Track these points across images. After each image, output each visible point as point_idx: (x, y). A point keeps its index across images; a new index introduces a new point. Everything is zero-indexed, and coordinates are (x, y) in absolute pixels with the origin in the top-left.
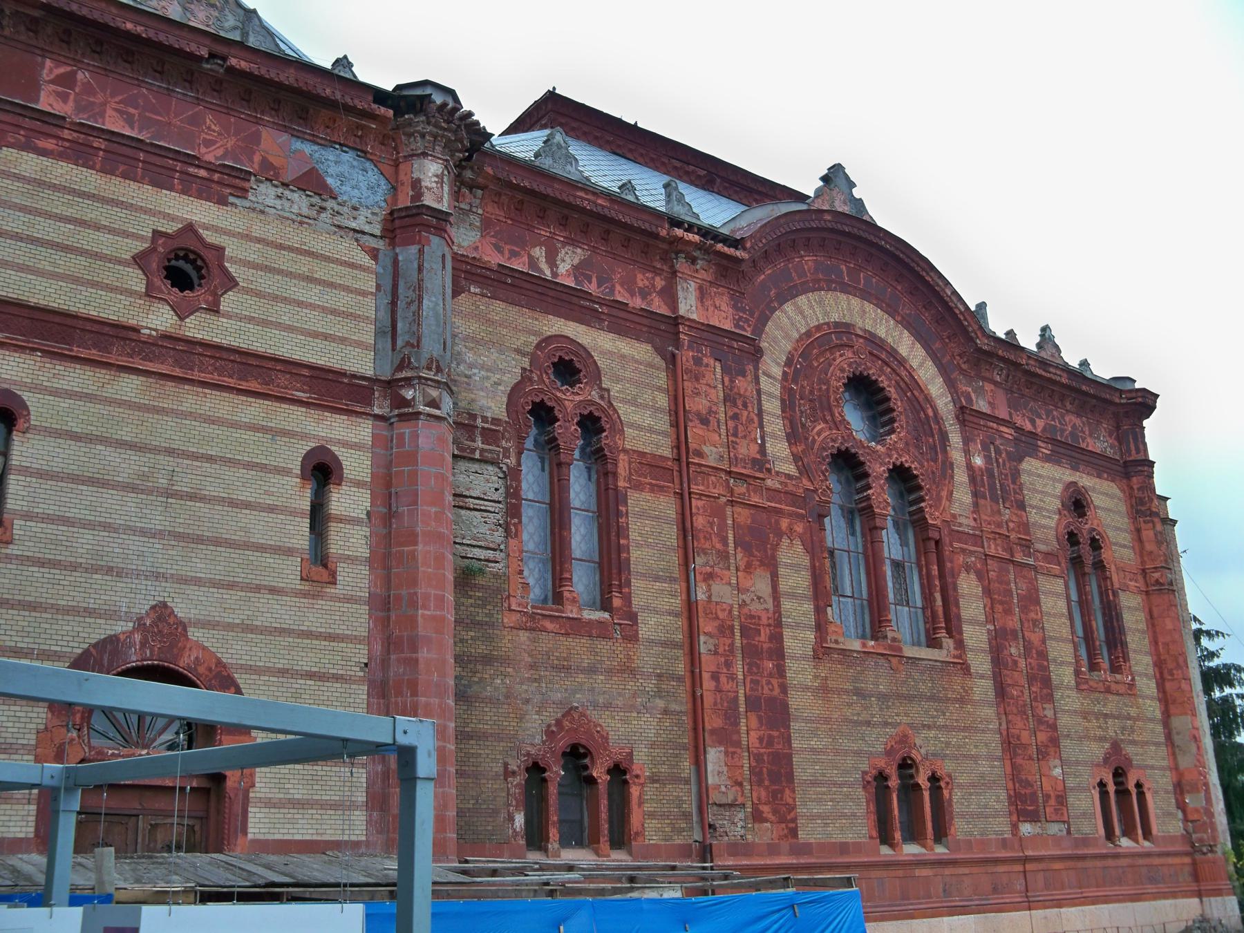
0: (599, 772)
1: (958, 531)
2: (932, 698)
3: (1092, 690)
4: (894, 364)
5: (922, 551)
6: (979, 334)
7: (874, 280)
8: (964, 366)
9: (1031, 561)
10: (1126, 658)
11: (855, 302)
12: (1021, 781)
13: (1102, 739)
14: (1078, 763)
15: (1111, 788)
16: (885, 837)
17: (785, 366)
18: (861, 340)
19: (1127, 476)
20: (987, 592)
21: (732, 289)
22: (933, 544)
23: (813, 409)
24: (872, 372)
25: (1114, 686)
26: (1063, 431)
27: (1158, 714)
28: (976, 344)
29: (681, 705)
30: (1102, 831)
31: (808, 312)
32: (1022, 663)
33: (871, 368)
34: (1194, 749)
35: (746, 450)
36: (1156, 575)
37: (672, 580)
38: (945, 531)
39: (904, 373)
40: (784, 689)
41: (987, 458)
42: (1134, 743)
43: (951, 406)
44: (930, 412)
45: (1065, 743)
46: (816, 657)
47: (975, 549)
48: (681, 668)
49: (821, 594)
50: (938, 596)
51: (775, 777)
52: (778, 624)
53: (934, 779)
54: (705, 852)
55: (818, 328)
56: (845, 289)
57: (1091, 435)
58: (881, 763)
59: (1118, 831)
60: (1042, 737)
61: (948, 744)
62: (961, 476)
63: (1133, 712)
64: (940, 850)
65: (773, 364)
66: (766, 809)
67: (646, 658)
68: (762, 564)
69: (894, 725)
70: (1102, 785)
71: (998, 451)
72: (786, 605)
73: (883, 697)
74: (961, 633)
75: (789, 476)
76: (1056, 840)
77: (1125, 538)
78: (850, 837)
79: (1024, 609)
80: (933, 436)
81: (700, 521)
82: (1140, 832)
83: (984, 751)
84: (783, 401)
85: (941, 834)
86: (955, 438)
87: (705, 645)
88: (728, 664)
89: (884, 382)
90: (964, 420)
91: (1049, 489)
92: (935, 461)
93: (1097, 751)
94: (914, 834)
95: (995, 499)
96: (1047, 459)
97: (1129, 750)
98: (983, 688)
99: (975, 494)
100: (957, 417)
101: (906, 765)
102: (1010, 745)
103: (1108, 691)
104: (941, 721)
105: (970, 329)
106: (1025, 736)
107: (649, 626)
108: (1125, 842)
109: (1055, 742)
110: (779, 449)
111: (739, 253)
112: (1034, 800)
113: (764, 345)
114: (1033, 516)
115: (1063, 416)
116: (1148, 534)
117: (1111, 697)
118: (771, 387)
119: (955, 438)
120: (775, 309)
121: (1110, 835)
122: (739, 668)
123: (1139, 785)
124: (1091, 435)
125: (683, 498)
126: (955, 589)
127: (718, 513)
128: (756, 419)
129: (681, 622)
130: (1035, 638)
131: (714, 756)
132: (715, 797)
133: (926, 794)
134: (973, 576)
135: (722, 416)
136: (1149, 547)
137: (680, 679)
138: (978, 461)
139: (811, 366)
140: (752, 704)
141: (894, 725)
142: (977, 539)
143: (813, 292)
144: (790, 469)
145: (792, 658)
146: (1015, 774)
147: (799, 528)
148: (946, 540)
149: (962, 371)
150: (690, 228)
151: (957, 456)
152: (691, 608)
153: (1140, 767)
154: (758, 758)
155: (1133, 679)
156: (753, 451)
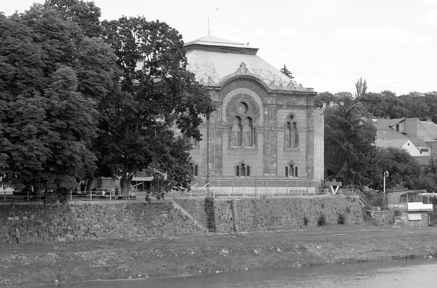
0: (194, 167)
2: (249, 154)
3: (287, 151)
5: (252, 130)
9: (276, 130)
10: (298, 145)
11: (243, 89)
12: (266, 167)
13: (288, 160)
14: (281, 164)
15: (289, 168)
16: (238, 175)
19: (308, 109)
20: (264, 136)
22: (254, 129)
23: (232, 110)
24: (245, 102)
25: (293, 150)
26: (291, 102)
27: (305, 155)
29: (206, 157)
30: (285, 175)
31: (233, 93)
32: (270, 148)
34: (311, 161)
35: (219, 120)
36: (309, 129)
37: (205, 140)
38: (256, 127)
39: (252, 100)
40: (222, 154)
41: (269, 112)
42: (297, 160)
43: (262, 104)
44: (256, 106)
45: (278, 160)
46: (228, 149)
48: (206, 152)
49: (230, 140)
50: (253, 138)
51: (219, 167)
52: (222, 145)
53: (248, 167)
54: (208, 177)
55: (234, 96)
56: (241, 87)
57: (299, 101)
58: (238, 165)
59: (294, 175)
60: (272, 160)
61: (251, 162)
62: (262, 116)
63: (297, 155)
64: (248, 177)
65: (225, 105)
66: (217, 171)
67: (201, 151)
68: (220, 137)
69: (241, 159)
70: (287, 168)
71: (272, 110)
72: (223, 142)
73: (240, 155)
74: (257, 143)
75: (226, 122)
76: (273, 177)
77: (305, 121)
78: (231, 175)
79: (272, 139)
81: (210, 132)
82: (294, 175)
83: (259, 162)
85: (248, 175)
86: (261, 110)
87: (209, 149)
88: (213, 152)
89: (247, 103)
91: (284, 115)
92: (256, 114)
93: (287, 162)
94: (244, 175)
95: (269, 119)
96: (285, 109)
97: (295, 162)
98: (260, 152)
99: (264, 119)
101: (243, 165)
102: (265, 161)
103: (292, 151)
104: (251, 158)
106: (268, 160)
107: (201, 147)
108: (291, 177)
109: (276, 161)
110: (225, 119)
111: (220, 89)
112: (269, 170)
113: (224, 101)
114: (279, 121)
115: (291, 99)
116: (309, 121)
117: (292, 152)
118: (224, 108)
119: (261, 110)
120: (226, 95)
121: (287, 175)
122: (215, 152)
123: (296, 168)
124: (299, 101)
125: (208, 129)
126: (257, 136)
127: (213, 130)
129: (206, 146)
130: (274, 143)
131: (210, 164)
132: (209, 169)
133: (246, 169)
134: (261, 134)
135: (215, 115)
136: (309, 123)
137: (206, 154)
138: (266, 113)
139: (232, 103)
140: (216, 157)
141: (241, 159)
142: (263, 127)
144: (227, 121)
145: (224, 150)
146: (265, 165)
147: (227, 130)
148: (256, 128)
149: (266, 96)
150: (211, 87)
151: (261, 112)
152: (208, 144)
153: (297, 164)
154: (217, 164)
155: (299, 149)
156: (220, 120)
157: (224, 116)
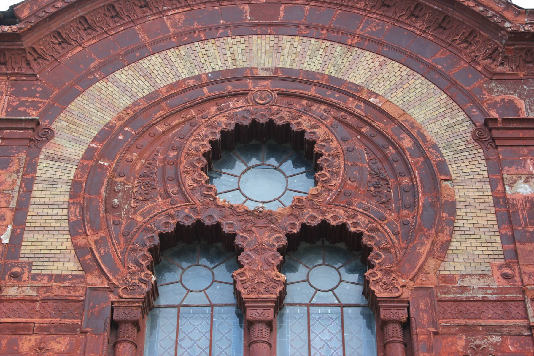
1: (455, 301)
4: (335, 98)
6: (508, 14)
7: (308, 7)
8: (506, 69)
17: (94, 140)
18: (266, 83)
21: (12, 75)
22: (395, 331)
28: (504, 29)
33: (279, 111)
39: (352, 105)
44: (407, 143)
47: (503, 322)
75: (60, 278)
80: (409, 172)
84: (76, 184)
90: (494, 140)
92: (413, 206)
100: (478, 138)
105: (490, 14)
128: (9, 215)
143: (176, 47)
149: (494, 76)
157: (44, 230)
